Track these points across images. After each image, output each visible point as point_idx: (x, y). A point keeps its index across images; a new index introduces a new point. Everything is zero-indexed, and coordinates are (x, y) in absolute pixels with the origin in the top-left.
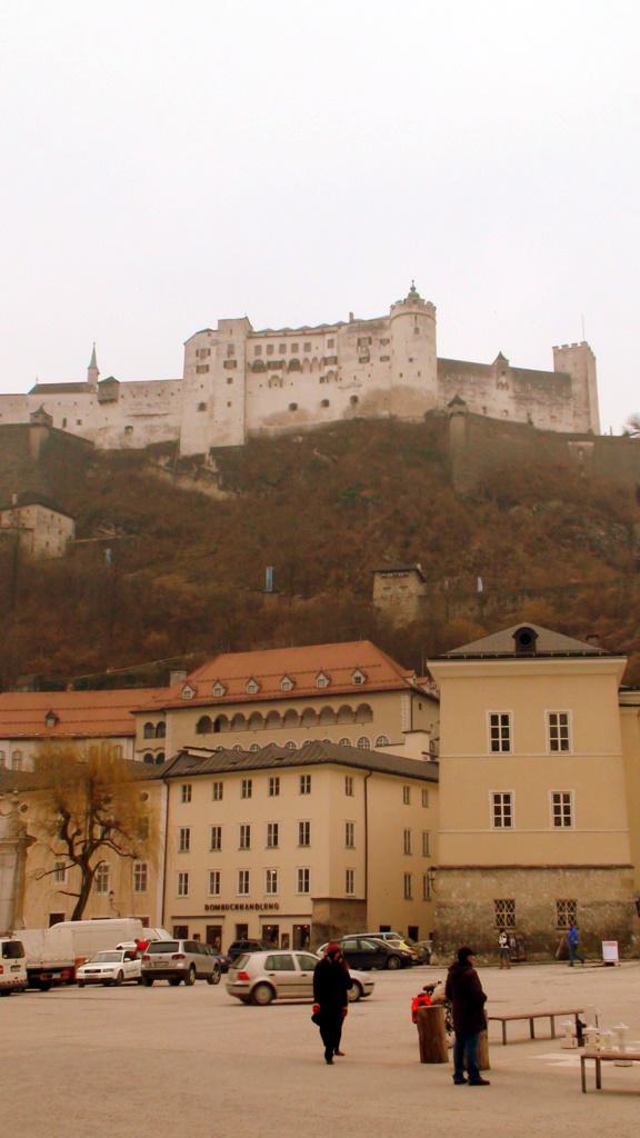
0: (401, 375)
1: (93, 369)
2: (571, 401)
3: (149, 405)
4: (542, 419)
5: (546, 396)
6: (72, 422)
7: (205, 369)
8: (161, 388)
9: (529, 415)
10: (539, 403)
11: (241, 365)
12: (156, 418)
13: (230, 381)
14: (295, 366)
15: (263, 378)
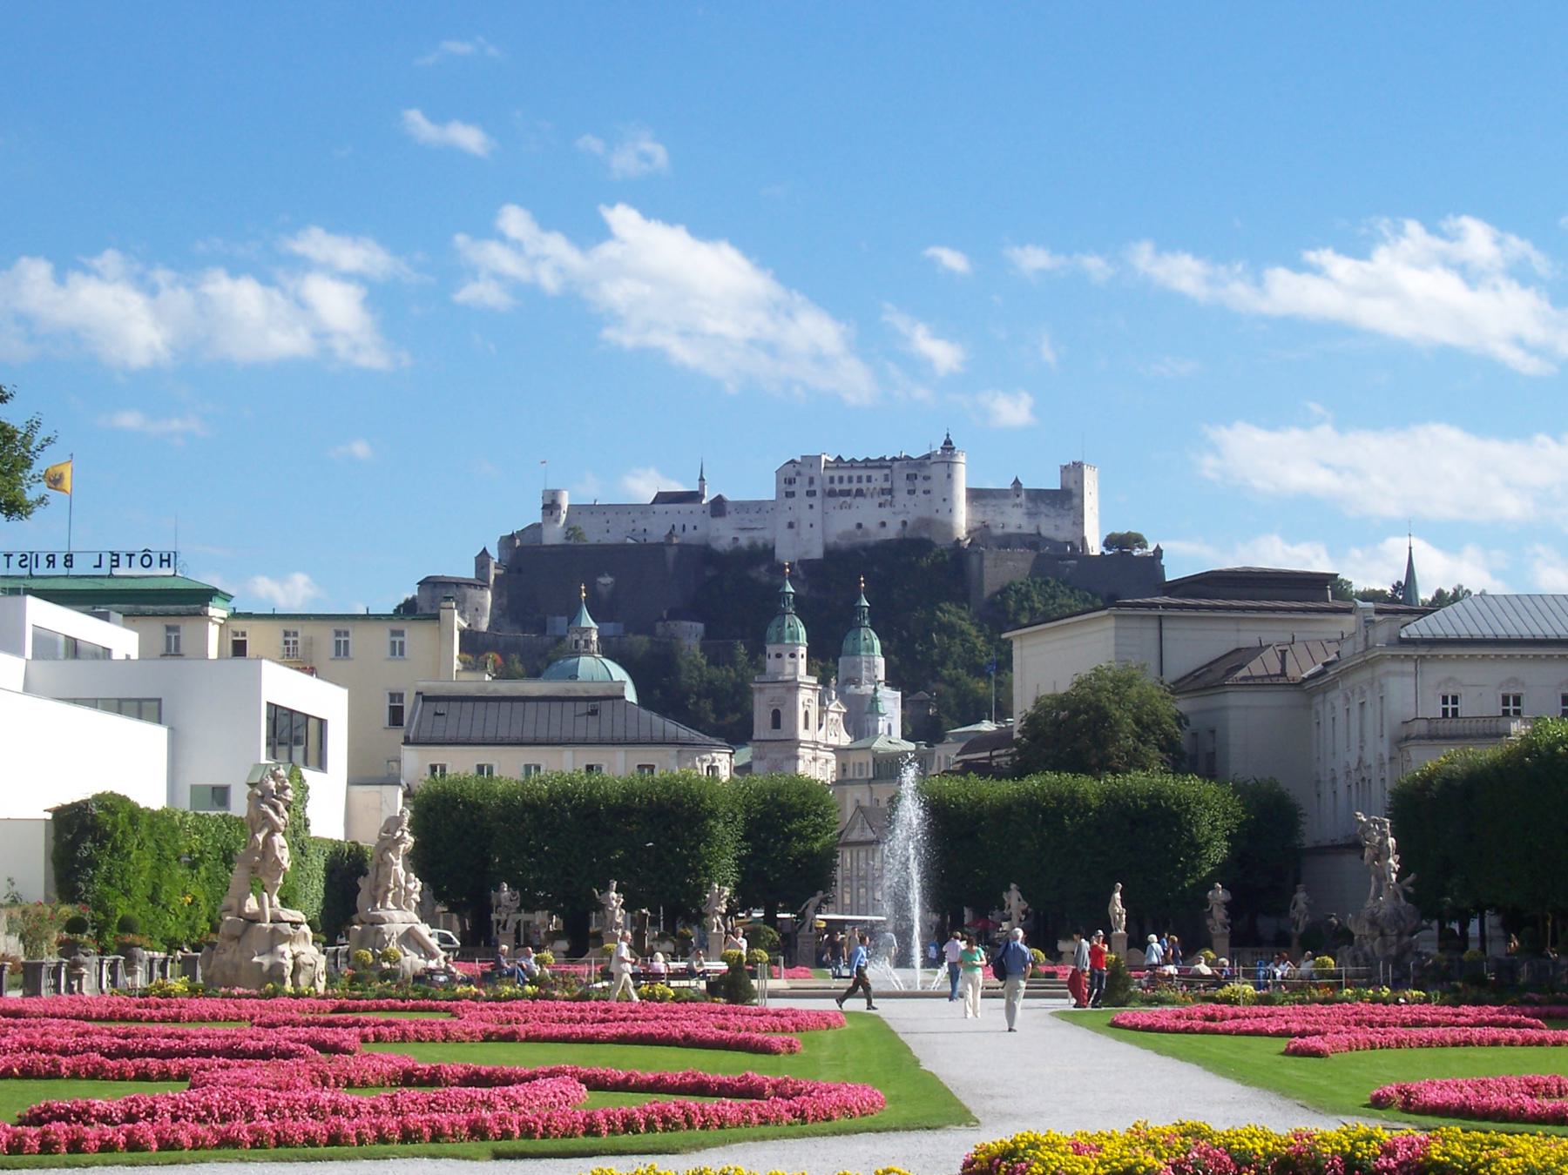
0: (937, 511)
1: (702, 479)
2: (1072, 512)
3: (751, 521)
4: (1048, 530)
5: (1052, 510)
6: (689, 528)
7: (790, 495)
8: (758, 506)
9: (1038, 527)
10: (1046, 515)
11: (819, 494)
12: (755, 531)
13: (811, 506)
14: (860, 493)
15: (833, 501)
